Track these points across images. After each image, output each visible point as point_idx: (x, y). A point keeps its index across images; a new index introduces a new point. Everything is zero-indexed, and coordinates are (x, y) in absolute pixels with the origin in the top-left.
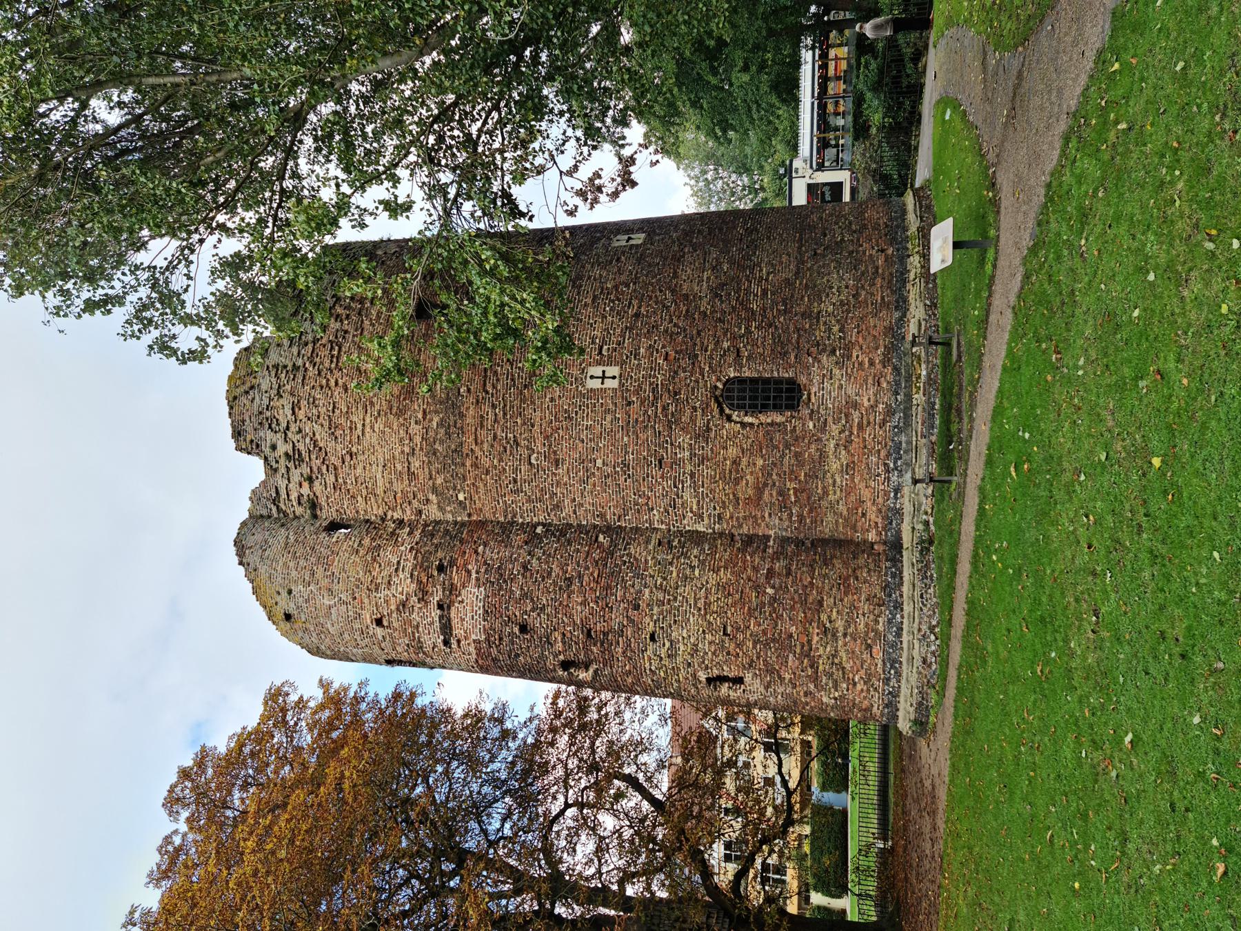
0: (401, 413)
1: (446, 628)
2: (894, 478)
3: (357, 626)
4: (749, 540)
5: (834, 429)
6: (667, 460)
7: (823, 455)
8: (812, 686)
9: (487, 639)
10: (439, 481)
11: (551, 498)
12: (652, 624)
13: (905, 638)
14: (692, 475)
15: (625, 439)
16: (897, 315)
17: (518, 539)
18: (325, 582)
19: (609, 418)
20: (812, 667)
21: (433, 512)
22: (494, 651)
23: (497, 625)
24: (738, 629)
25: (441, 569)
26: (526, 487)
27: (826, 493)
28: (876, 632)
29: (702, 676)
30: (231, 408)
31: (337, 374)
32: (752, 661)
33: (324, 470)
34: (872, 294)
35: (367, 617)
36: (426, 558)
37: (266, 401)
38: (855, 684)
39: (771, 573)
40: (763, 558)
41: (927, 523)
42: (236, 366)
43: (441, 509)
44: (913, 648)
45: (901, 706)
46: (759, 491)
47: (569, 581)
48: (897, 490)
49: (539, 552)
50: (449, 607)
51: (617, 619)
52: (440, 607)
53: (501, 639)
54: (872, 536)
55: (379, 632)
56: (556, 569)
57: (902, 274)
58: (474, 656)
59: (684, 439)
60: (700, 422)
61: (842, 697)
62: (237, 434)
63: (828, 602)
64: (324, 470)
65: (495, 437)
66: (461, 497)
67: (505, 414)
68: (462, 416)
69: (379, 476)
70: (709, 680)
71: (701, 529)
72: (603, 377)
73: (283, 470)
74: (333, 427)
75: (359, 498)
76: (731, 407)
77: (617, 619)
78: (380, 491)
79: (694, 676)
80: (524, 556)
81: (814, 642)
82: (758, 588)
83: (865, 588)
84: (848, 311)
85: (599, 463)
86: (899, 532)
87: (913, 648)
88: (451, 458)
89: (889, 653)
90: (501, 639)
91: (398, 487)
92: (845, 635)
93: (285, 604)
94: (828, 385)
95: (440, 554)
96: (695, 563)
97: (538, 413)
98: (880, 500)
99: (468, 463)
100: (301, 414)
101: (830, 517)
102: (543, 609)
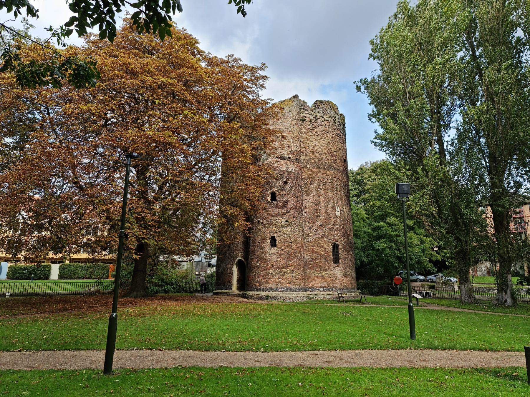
1: (283, 158)
2: (322, 289)
5: (331, 273)
7: (326, 270)
10: (312, 161)
13: (293, 293)
14: (319, 234)
22: (277, 172)
27: (317, 271)
29: (276, 235)
30: (327, 101)
35: (284, 134)
37: (329, 113)
41: (313, 298)
42: (335, 105)
43: (304, 160)
44: (293, 295)
45: (271, 292)
46: (316, 253)
48: (319, 290)
51: (291, 211)
52: (289, 158)
59: (327, 233)
60: (331, 237)
62: (321, 102)
66: (308, 166)
68: (328, 170)
70: (274, 237)
71: (305, 236)
73: (313, 114)
74: (323, 131)
77: (291, 211)
79: (275, 233)
82: (299, 252)
85: (320, 208)
86: (308, 291)
87: (293, 295)
88: (318, 165)
91: (310, 148)
93: (286, 109)
94: (339, 271)
99: (317, 170)
101: (310, 272)
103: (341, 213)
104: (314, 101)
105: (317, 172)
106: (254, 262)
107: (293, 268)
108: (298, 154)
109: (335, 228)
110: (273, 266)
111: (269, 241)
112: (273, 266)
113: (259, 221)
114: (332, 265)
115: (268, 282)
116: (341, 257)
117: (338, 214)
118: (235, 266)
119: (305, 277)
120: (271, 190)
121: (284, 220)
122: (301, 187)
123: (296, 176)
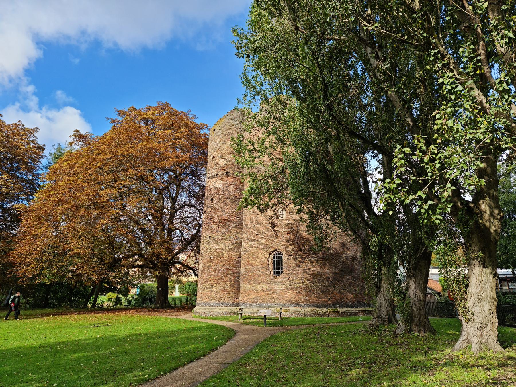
1: (212, 177)
4: (239, 263)
5: (267, 286)
6: (259, 236)
7: (260, 283)
14: (255, 244)
16: (303, 305)
17: (237, 194)
18: (222, 139)
23: (213, 192)
25: (227, 173)
27: (250, 284)
28: (212, 300)
34: (311, 297)
36: (230, 168)
39: (228, 269)
40: (232, 267)
46: (251, 265)
47: (224, 211)
49: (233, 201)
51: (214, 226)
52: (217, 175)
54: (241, 298)
55: (212, 158)
56: (227, 207)
57: (319, 306)
59: (264, 241)
60: (269, 245)
63: (219, 286)
72: (282, 214)
77: (214, 226)
80: (231, 197)
82: (223, 265)
83: (223, 296)
84: (304, 289)
85: (258, 216)
94: (280, 283)
95: (231, 172)
96: (230, 247)
101: (245, 286)
102: (217, 205)
107: (212, 282)
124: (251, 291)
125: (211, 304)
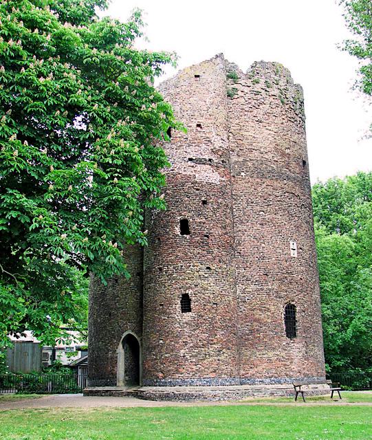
0: (276, 149)
1: (200, 161)
2: (268, 380)
3: (196, 113)
8: (191, 345)
9: (196, 182)
11: (246, 220)
12: (214, 268)
15: (274, 259)
19: (281, 251)
20: (203, 345)
21: (234, 158)
24: (216, 310)
26: (249, 208)
29: (189, 292)
31: (286, 120)
32: (202, 317)
33: (250, 106)
35: (201, 121)
38: (196, 365)
43: (236, 162)
46: (258, 320)
50: (210, 165)
51: (216, 251)
52: (210, 160)
53: (197, 190)
55: (195, 125)
58: (184, 173)
60: (283, 294)
61: (187, 360)
64: (250, 106)
65: (270, 195)
66: (242, 174)
67: (279, 201)
69: (250, 134)
75: (238, 121)
76: (286, 308)
78: (242, 132)
79: (189, 288)
81: (214, 346)
85: (263, 245)
88: (261, 173)
89: (213, 380)
90: (197, 190)
92: (219, 360)
94: (296, 348)
97: (280, 217)
98: (258, 375)
99: (259, 180)
100: (271, 99)
103: (298, 253)
104: (252, 62)
105: (257, 183)
106: (154, 339)
108: (224, 154)
109: (289, 278)
110: (186, 343)
111: (179, 302)
112: (186, 343)
113: (160, 269)
114: (285, 340)
115: (177, 371)
116: (299, 326)
117: (294, 254)
118: (121, 346)
119: (238, 361)
120: (180, 215)
121: (203, 266)
122: (232, 209)
123: (222, 191)
124: (261, 360)
125: (220, 380)
